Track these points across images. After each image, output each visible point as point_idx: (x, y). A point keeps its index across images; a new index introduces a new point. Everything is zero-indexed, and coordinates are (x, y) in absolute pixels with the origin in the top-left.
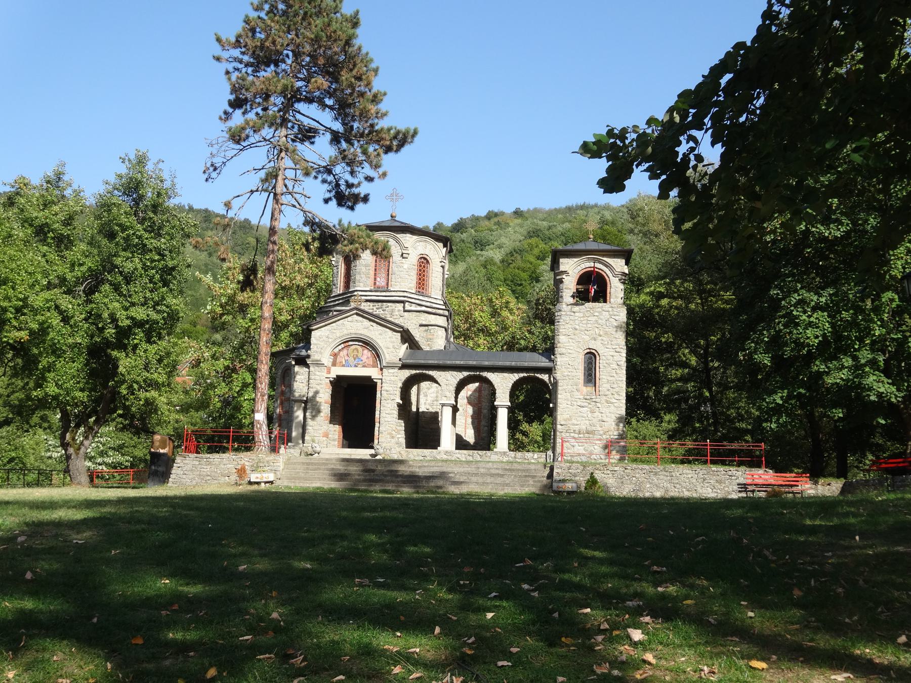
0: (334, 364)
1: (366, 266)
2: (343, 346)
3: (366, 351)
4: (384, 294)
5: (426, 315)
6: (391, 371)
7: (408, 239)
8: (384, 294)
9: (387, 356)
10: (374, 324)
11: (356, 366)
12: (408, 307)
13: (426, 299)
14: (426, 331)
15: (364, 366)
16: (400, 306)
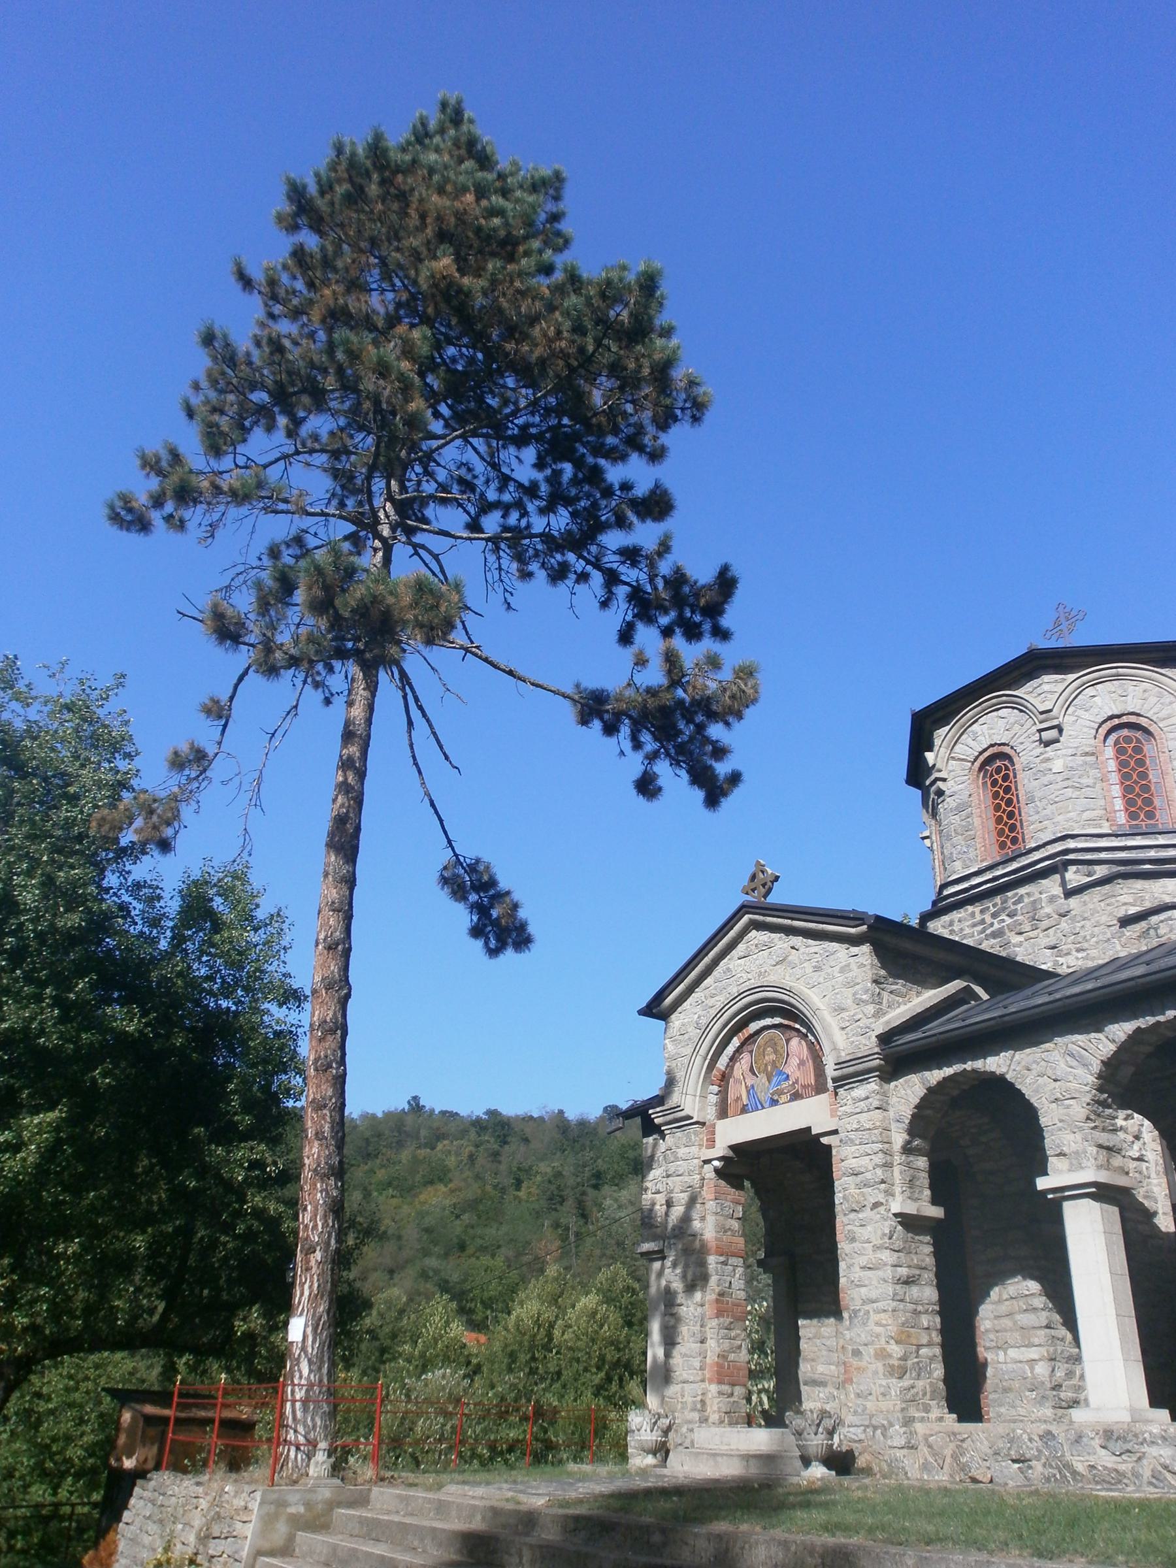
0: (723, 1113)
1: (959, 809)
2: (736, 1042)
3: (795, 1042)
4: (1015, 865)
5: (1139, 884)
6: (860, 1091)
7: (1045, 690)
8: (1015, 865)
9: (840, 1038)
10: (798, 941)
11: (774, 1103)
12: (1074, 877)
13: (1161, 840)
14: (1145, 934)
15: (796, 1096)
16: (1051, 886)
